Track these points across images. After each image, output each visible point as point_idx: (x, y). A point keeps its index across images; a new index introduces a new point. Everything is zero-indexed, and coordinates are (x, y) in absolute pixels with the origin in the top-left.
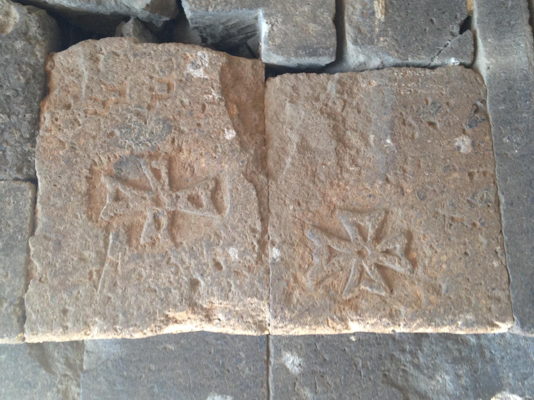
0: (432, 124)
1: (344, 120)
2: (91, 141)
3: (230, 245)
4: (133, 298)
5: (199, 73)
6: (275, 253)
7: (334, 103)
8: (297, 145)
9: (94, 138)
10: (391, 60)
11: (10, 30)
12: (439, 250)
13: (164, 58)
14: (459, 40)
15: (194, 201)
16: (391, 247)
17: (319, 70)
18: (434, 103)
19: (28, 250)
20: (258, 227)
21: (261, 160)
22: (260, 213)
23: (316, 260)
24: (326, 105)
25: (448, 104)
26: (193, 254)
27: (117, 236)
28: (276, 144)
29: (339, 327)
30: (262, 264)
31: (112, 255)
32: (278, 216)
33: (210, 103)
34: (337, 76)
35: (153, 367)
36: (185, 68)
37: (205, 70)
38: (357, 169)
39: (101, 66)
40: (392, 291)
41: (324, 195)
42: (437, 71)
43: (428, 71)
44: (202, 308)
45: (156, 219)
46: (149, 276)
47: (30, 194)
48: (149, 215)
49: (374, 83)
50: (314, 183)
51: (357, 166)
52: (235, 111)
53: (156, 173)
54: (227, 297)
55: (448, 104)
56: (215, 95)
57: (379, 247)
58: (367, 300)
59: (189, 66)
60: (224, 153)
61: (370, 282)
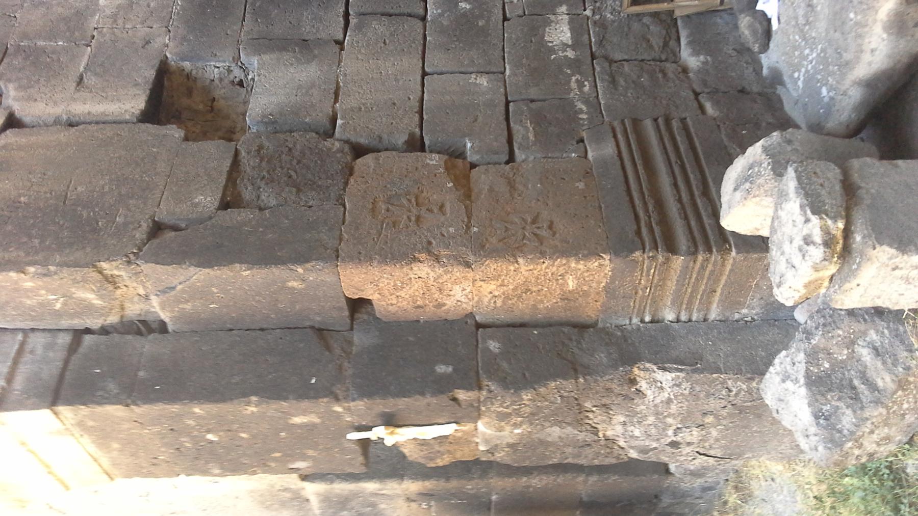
20: (466, 220)
21: (468, 196)
35: (399, 350)
40: (542, 244)
45: (409, 218)
53: (409, 201)
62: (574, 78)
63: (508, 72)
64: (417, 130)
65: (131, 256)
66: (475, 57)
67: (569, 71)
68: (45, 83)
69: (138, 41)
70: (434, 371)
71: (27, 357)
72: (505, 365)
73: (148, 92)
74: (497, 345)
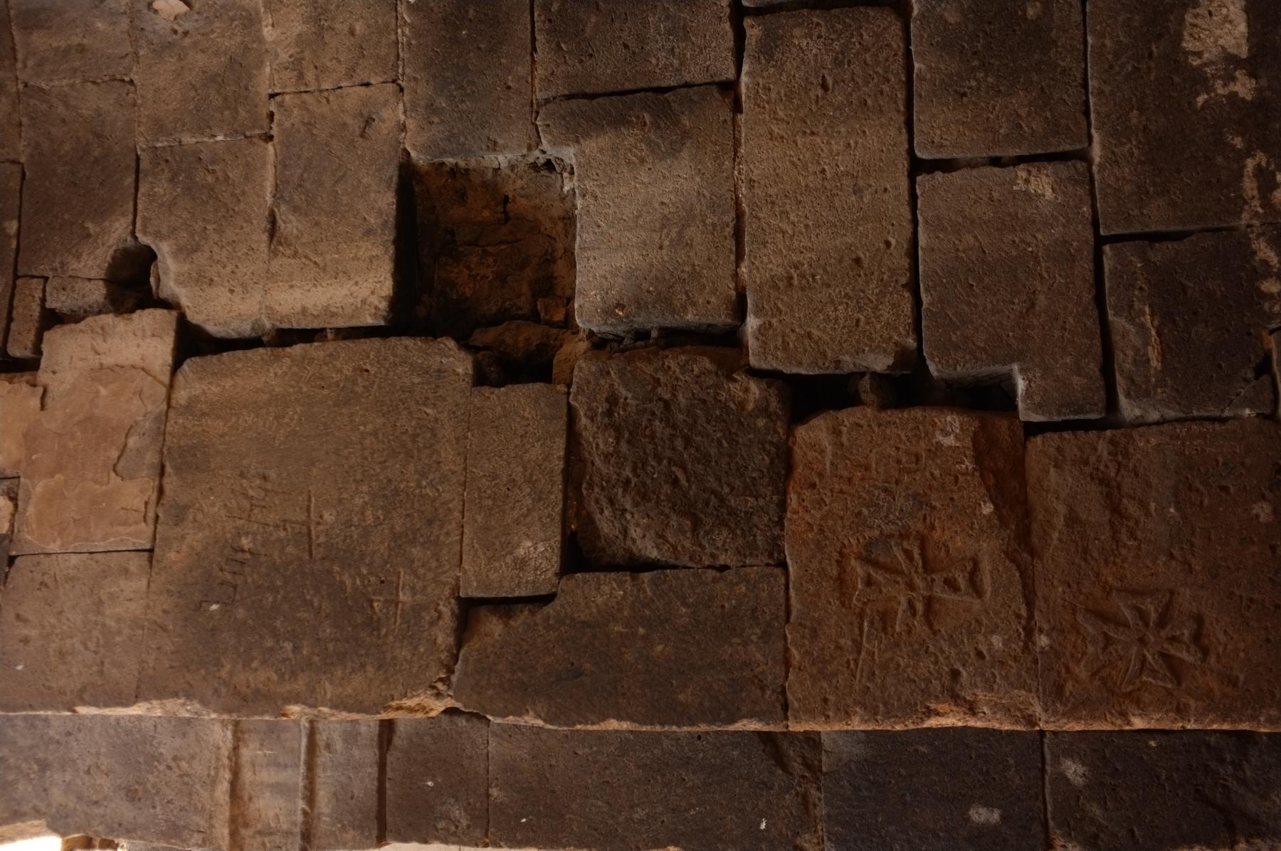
0: (1225, 489)
1: (1119, 486)
2: (839, 522)
3: (993, 632)
4: (893, 689)
5: (949, 441)
6: (1043, 641)
7: (1106, 466)
8: (1065, 517)
9: (842, 518)
10: (1171, 414)
11: (751, 406)
12: (1235, 636)
13: (910, 426)
14: (1254, 387)
15: (951, 584)
16: (1178, 633)
17: (1086, 426)
18: (1225, 464)
19: (785, 638)
20: (1024, 613)
21: (1024, 536)
22: (1025, 596)
23: (1091, 649)
24: (1097, 469)
25: (1242, 464)
26: (952, 643)
27: (872, 624)
28: (1040, 517)
29: (1119, 722)
30: (1030, 653)
31: (869, 642)
32: (1046, 599)
33: (963, 474)
34: (1108, 433)
35: (903, 772)
36: (934, 436)
37: (956, 437)
38: (1136, 543)
39: (844, 439)
40: (1179, 683)
41: (1098, 575)
42: (1230, 425)
43: (1217, 426)
44: (965, 700)
46: (908, 666)
47: (782, 580)
48: (903, 600)
49: (1153, 441)
50: (1086, 561)
51: (1135, 539)
52: (992, 481)
53: (908, 555)
54: (992, 689)
55: (1242, 464)
56: (968, 464)
57: (1163, 633)
58: (1150, 693)
59: (938, 433)
60: (981, 530)
61: (1154, 673)
62: (1250, 164)
63: (1097, 153)
64: (911, 342)
65: (440, 686)
66: (1023, 112)
67: (1238, 142)
68: (216, 237)
69: (349, 121)
70: (967, 820)
71: (323, 758)
72: (1096, 810)
73: (392, 250)
74: (1081, 770)
